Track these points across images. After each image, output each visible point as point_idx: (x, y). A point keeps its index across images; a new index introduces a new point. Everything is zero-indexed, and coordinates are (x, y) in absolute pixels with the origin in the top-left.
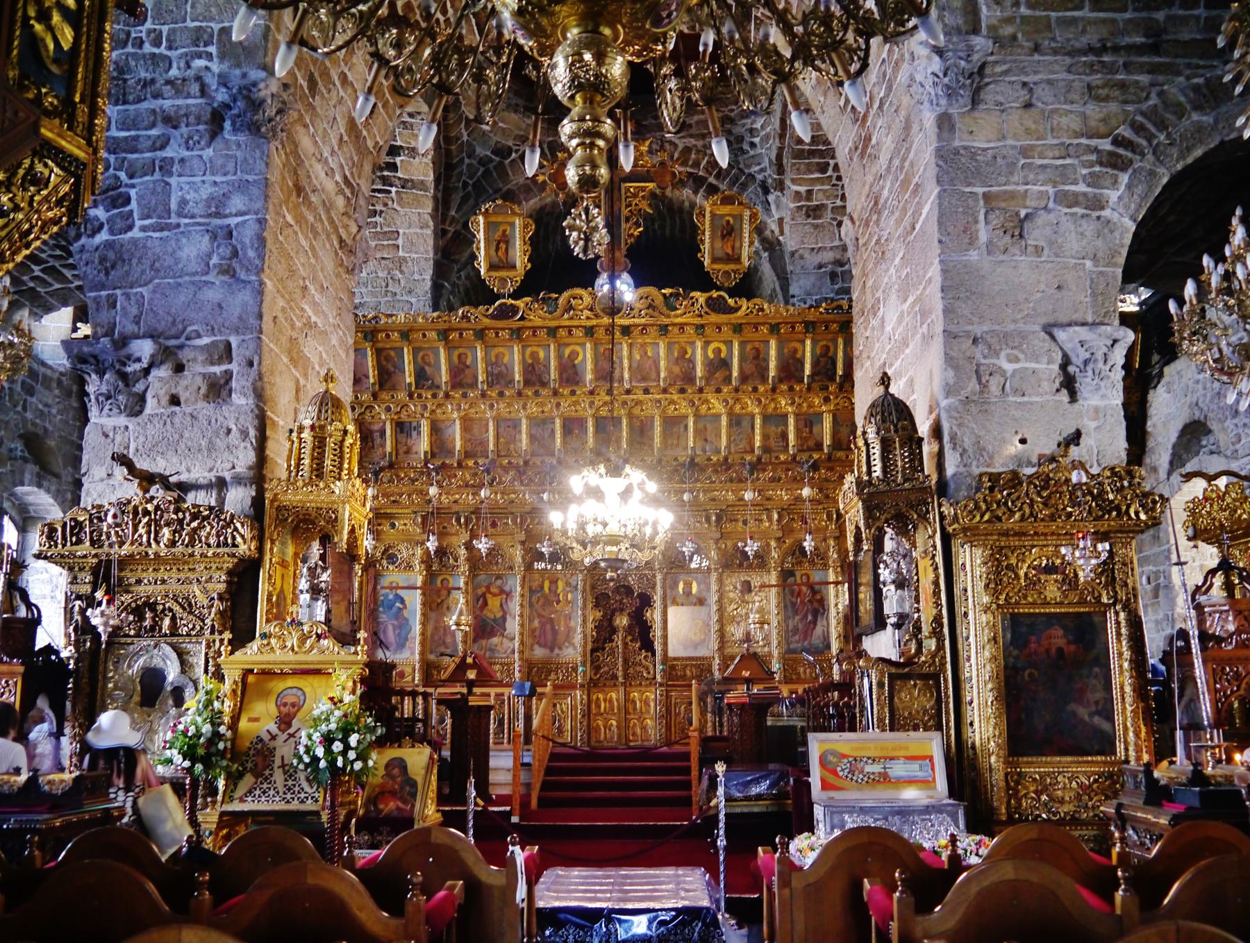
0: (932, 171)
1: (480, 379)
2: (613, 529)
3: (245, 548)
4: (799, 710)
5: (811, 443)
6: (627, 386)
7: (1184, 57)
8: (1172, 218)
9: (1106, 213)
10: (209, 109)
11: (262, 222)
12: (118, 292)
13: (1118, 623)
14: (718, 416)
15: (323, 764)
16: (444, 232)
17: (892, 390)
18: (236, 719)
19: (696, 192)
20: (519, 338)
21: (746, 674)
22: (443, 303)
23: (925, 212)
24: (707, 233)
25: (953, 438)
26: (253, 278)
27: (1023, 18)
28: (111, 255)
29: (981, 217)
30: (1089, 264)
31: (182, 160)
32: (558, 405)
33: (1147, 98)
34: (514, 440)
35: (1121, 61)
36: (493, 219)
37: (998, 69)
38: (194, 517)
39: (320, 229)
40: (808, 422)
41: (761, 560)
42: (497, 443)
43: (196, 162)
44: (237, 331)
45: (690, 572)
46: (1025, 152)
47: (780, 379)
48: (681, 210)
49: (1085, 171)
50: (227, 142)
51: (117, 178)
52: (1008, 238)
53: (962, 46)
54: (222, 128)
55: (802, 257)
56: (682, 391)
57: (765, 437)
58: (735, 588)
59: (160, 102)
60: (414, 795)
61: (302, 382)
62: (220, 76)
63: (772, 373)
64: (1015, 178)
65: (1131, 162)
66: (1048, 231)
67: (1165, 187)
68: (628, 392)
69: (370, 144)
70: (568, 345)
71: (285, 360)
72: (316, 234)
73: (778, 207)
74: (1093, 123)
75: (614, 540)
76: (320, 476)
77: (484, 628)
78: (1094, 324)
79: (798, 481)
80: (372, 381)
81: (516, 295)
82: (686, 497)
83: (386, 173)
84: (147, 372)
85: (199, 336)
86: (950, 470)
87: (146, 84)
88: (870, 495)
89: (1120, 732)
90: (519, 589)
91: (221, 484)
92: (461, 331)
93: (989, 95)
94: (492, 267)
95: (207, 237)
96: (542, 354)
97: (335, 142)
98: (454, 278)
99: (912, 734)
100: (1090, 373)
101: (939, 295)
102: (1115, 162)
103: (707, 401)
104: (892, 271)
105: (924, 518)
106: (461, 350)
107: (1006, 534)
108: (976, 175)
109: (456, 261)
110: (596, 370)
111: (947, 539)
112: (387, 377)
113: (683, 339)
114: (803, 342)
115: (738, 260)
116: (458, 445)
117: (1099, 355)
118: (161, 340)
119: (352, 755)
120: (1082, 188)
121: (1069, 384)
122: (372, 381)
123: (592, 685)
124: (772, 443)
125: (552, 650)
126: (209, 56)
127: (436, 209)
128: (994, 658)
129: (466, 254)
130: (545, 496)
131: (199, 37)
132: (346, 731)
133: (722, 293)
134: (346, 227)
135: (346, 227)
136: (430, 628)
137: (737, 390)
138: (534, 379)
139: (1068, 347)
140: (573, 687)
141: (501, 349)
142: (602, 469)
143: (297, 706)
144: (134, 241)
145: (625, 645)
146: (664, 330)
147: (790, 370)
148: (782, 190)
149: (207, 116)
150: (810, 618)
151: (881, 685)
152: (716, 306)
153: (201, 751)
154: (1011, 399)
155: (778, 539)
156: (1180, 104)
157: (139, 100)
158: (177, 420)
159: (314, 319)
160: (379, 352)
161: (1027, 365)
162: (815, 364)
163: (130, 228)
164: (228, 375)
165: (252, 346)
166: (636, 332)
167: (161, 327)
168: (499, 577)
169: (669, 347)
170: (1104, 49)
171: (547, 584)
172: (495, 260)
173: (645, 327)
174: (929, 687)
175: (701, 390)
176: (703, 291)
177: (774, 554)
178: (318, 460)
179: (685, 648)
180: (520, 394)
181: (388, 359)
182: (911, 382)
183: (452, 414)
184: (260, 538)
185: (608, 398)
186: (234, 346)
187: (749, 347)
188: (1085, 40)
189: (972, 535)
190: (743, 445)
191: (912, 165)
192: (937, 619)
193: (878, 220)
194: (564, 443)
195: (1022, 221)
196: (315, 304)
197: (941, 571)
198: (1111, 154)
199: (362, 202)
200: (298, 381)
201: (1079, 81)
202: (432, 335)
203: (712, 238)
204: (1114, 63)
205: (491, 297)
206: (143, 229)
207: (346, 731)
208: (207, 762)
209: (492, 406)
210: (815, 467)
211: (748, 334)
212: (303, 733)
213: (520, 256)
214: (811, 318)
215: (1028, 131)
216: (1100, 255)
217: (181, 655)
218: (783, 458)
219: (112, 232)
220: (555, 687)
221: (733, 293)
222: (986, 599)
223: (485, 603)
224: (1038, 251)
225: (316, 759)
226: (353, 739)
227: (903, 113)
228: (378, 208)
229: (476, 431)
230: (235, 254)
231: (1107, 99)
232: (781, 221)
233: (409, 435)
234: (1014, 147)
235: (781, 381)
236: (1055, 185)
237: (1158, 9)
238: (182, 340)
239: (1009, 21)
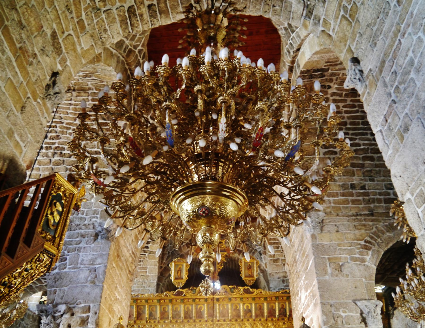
0: (311, 251)
1: (170, 316)
6: (218, 319)
7: (381, 217)
8: (387, 264)
9: (366, 263)
10: (95, 233)
11: (106, 267)
12: (58, 289)
16: (161, 267)
17: (306, 323)
19: (239, 255)
20: (183, 302)
22: (160, 290)
23: (310, 263)
24: (243, 268)
26: (101, 284)
27: (333, 207)
28: (58, 277)
29: (328, 265)
30: (364, 280)
31: (84, 248)
32: (195, 325)
33: (372, 229)
35: (363, 218)
36: (177, 264)
37: (327, 221)
39: (123, 268)
43: (88, 248)
44: (93, 302)
46: (339, 245)
47: (268, 316)
48: (235, 260)
50: (99, 242)
51: (64, 253)
52: (337, 272)
53: (316, 215)
54: (97, 238)
55: (273, 275)
56: (236, 320)
59: (81, 230)
61: (112, 319)
62: (100, 223)
63: (266, 314)
64: (337, 253)
65: (371, 248)
66: (349, 269)
67: (383, 255)
68: (218, 321)
70: (199, 304)
71: (107, 311)
72: (122, 269)
73: (265, 259)
74: (358, 236)
78: (369, 300)
80: (134, 316)
81: (183, 288)
83: (145, 249)
84: (62, 316)
85: (81, 304)
87: (77, 225)
92: (164, 299)
93: (326, 228)
94: (176, 279)
95: (88, 271)
96: (190, 308)
97: (131, 241)
98: (163, 282)
100: (370, 317)
101: (318, 290)
102: (367, 248)
103: (244, 324)
104: (302, 281)
106: (164, 306)
108: (324, 252)
109: (164, 276)
110: (208, 313)
112: (139, 315)
113: (236, 302)
114: (275, 303)
115: (253, 276)
117: (372, 310)
118: (68, 305)
120: (357, 256)
121: (364, 320)
122: (134, 316)
126: (97, 218)
127: (159, 260)
129: (168, 274)
131: (95, 212)
133: (248, 287)
134: (131, 267)
135: (131, 267)
137: (254, 320)
138: (188, 316)
141: (177, 306)
144: (66, 272)
146: (230, 299)
147: (271, 313)
148: (266, 254)
149: (94, 234)
152: (247, 292)
154: (346, 326)
156: (382, 230)
157: (75, 230)
159: (118, 297)
160: (138, 307)
161: (349, 314)
162: (280, 311)
163: (65, 268)
164: (88, 317)
165: (97, 307)
166: (221, 300)
167: (69, 301)
169: (232, 305)
170: (357, 215)
172: (177, 276)
173: (224, 298)
175: (242, 320)
176: (243, 286)
180: (183, 321)
181: (140, 309)
182: (312, 319)
185: (212, 323)
186: (91, 307)
187: (258, 305)
188: (351, 213)
191: (305, 249)
193: (296, 265)
195: (341, 267)
196: (119, 292)
198: (365, 245)
199: (137, 259)
200: (110, 319)
201: (352, 224)
202: (155, 301)
203: (245, 270)
204: (361, 219)
205: (175, 289)
206: (69, 268)
209: (173, 326)
211: (257, 300)
213: (185, 275)
214: (277, 295)
215: (339, 239)
216: (367, 277)
219: (59, 269)
221: (252, 287)
224: (347, 276)
227: (301, 233)
228: (142, 260)
230: (96, 277)
231: (360, 229)
232: (266, 264)
234: (335, 244)
235: (269, 317)
236: (349, 255)
237: (371, 204)
238: (75, 305)
239: (328, 207)
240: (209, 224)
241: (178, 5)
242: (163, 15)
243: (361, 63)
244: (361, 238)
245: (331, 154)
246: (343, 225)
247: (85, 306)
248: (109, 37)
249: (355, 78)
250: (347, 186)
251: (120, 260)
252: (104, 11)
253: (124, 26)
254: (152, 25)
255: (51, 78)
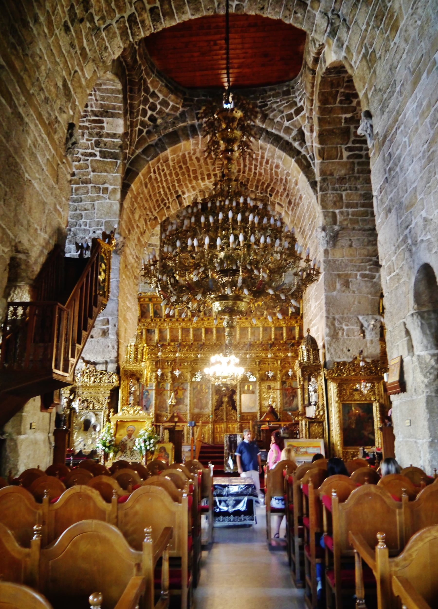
2: (225, 374)
3: (116, 384)
4: (286, 431)
5: (292, 337)
9: (375, 280)
14: (259, 328)
15: (143, 448)
18: (115, 435)
21: (268, 419)
25: (328, 349)
27: (350, 219)
30: (369, 296)
34: (188, 335)
38: (101, 374)
40: (290, 329)
41: (274, 378)
42: (182, 337)
44: (111, 315)
45: (250, 382)
46: (351, 261)
49: (368, 267)
57: (276, 335)
60: (168, 457)
69: (143, 242)
75: (225, 378)
76: (137, 361)
77: (179, 401)
79: (287, 350)
82: (248, 356)
86: (327, 359)
88: (304, 367)
89: (376, 439)
90: (189, 388)
91: (106, 363)
97: (134, 246)
99: (315, 440)
105: (319, 374)
107: (342, 380)
111: (326, 381)
116: (168, 337)
119: (152, 446)
120: (367, 272)
123: (215, 422)
124: (278, 337)
125: (201, 409)
128: (339, 417)
130: (199, 356)
132: (150, 438)
136: (158, 402)
139: (362, 321)
140: (207, 423)
142: (221, 354)
143: (133, 431)
145: (227, 408)
151: (306, 425)
153: (108, 445)
155: (280, 371)
158: (93, 343)
164: (108, 329)
165: (116, 320)
168: (182, 384)
171: (199, 386)
174: (319, 426)
177: (279, 376)
178: (136, 355)
181: (144, 307)
183: (167, 327)
184: (120, 380)
186: (110, 320)
189: (333, 380)
190: (268, 338)
192: (323, 405)
194: (205, 337)
197: (324, 390)
207: (150, 438)
208: (109, 447)
210: (293, 345)
212: (137, 440)
217: (96, 415)
218: (282, 342)
220: (203, 423)
222: (337, 399)
223: (177, 393)
225: (141, 447)
226: (152, 441)
229: (174, 332)
233: (151, 334)
239: (345, 220)
240: (231, 316)
241: (184, 4)
242: (167, 17)
243: (373, 118)
244: (374, 254)
245: (355, 158)
246: (358, 240)
247: (104, 319)
248: (110, 55)
249: (366, 131)
250: (368, 196)
251: (128, 270)
252: (104, 29)
253: (124, 38)
254: (155, 29)
255: (68, 130)
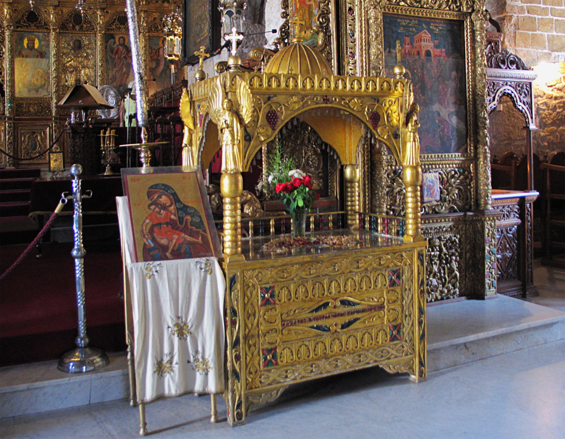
13: (473, 32)
58: (69, 45)
150: (124, 70)
155: (102, 9)
179: (29, 91)
